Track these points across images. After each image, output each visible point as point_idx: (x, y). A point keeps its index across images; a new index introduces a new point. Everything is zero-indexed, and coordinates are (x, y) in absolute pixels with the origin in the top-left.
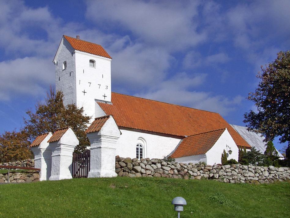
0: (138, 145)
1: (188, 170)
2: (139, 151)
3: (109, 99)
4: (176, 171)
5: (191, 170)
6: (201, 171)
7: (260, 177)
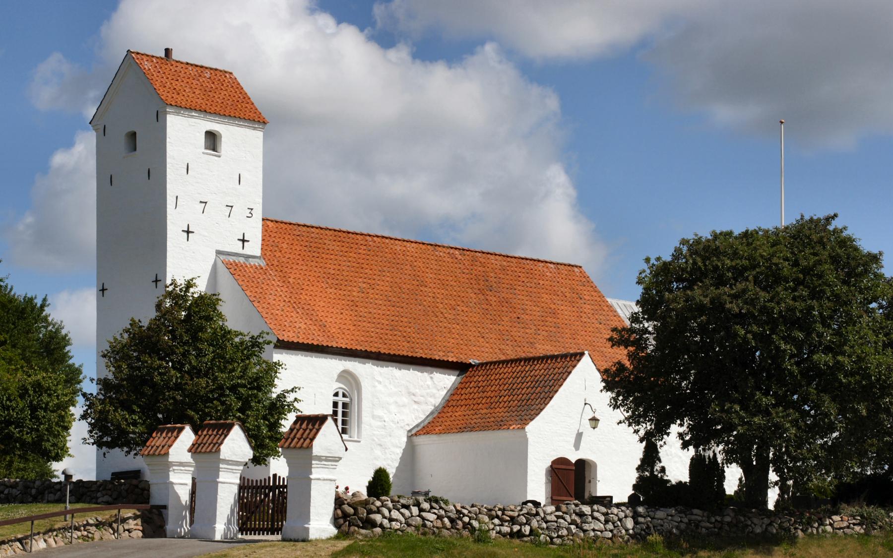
0: (336, 395)
1: (470, 518)
2: (340, 410)
3: (254, 248)
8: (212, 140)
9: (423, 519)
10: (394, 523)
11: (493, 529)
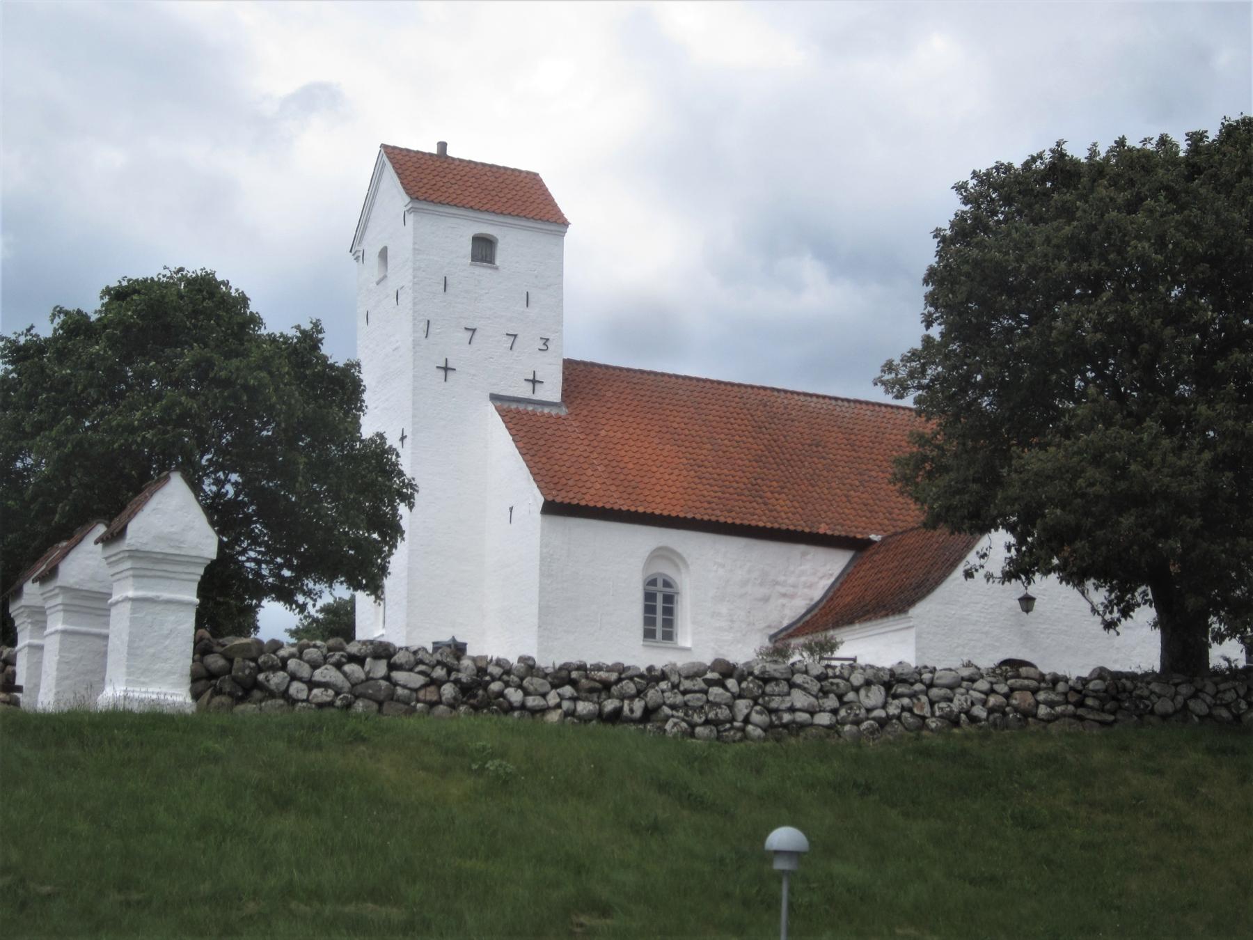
0: (653, 582)
2: (659, 604)
4: (448, 690)
5: (520, 687)
6: (568, 690)
7: (843, 713)
8: (484, 249)
9: (395, 684)
10: (315, 691)
11: (559, 706)
